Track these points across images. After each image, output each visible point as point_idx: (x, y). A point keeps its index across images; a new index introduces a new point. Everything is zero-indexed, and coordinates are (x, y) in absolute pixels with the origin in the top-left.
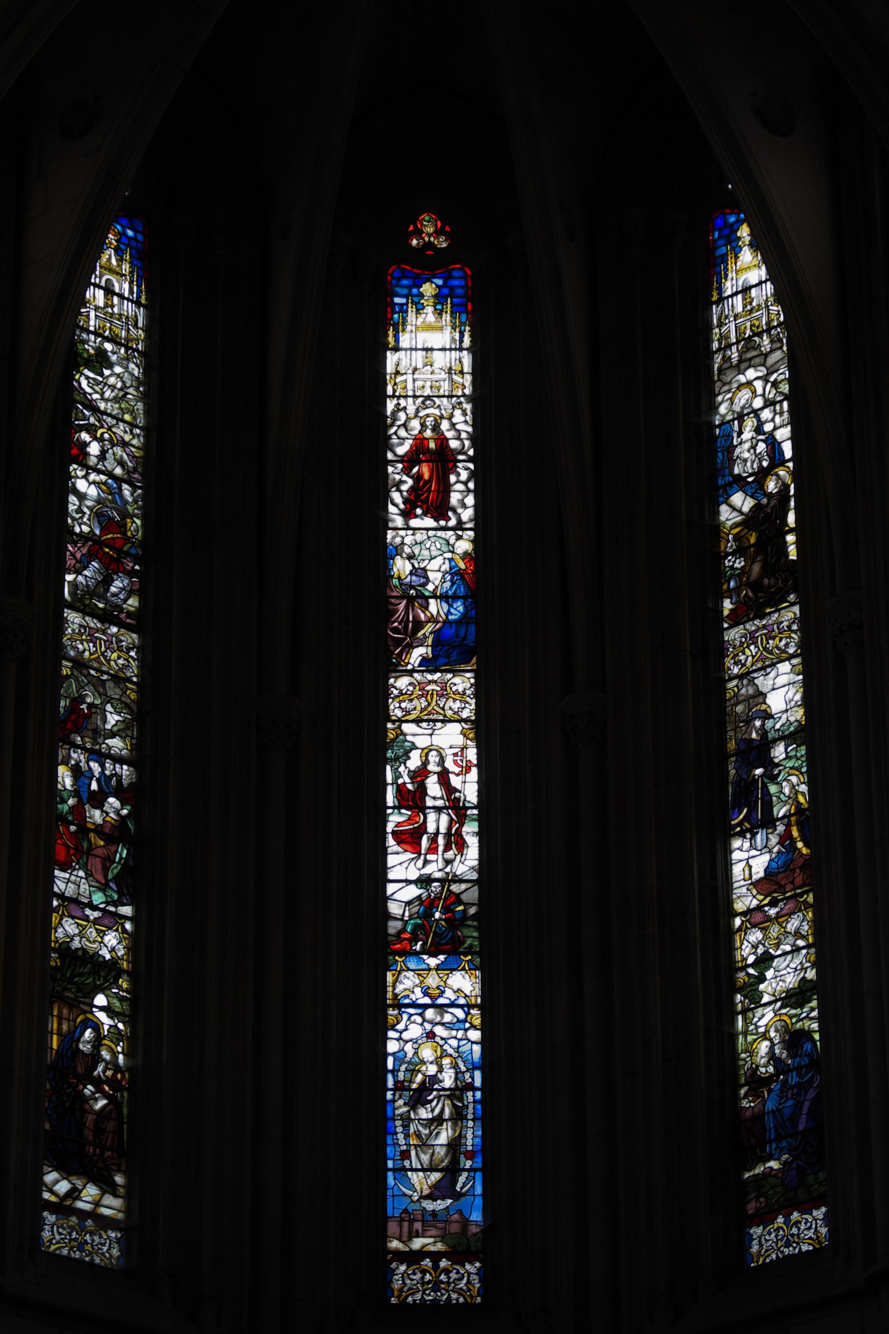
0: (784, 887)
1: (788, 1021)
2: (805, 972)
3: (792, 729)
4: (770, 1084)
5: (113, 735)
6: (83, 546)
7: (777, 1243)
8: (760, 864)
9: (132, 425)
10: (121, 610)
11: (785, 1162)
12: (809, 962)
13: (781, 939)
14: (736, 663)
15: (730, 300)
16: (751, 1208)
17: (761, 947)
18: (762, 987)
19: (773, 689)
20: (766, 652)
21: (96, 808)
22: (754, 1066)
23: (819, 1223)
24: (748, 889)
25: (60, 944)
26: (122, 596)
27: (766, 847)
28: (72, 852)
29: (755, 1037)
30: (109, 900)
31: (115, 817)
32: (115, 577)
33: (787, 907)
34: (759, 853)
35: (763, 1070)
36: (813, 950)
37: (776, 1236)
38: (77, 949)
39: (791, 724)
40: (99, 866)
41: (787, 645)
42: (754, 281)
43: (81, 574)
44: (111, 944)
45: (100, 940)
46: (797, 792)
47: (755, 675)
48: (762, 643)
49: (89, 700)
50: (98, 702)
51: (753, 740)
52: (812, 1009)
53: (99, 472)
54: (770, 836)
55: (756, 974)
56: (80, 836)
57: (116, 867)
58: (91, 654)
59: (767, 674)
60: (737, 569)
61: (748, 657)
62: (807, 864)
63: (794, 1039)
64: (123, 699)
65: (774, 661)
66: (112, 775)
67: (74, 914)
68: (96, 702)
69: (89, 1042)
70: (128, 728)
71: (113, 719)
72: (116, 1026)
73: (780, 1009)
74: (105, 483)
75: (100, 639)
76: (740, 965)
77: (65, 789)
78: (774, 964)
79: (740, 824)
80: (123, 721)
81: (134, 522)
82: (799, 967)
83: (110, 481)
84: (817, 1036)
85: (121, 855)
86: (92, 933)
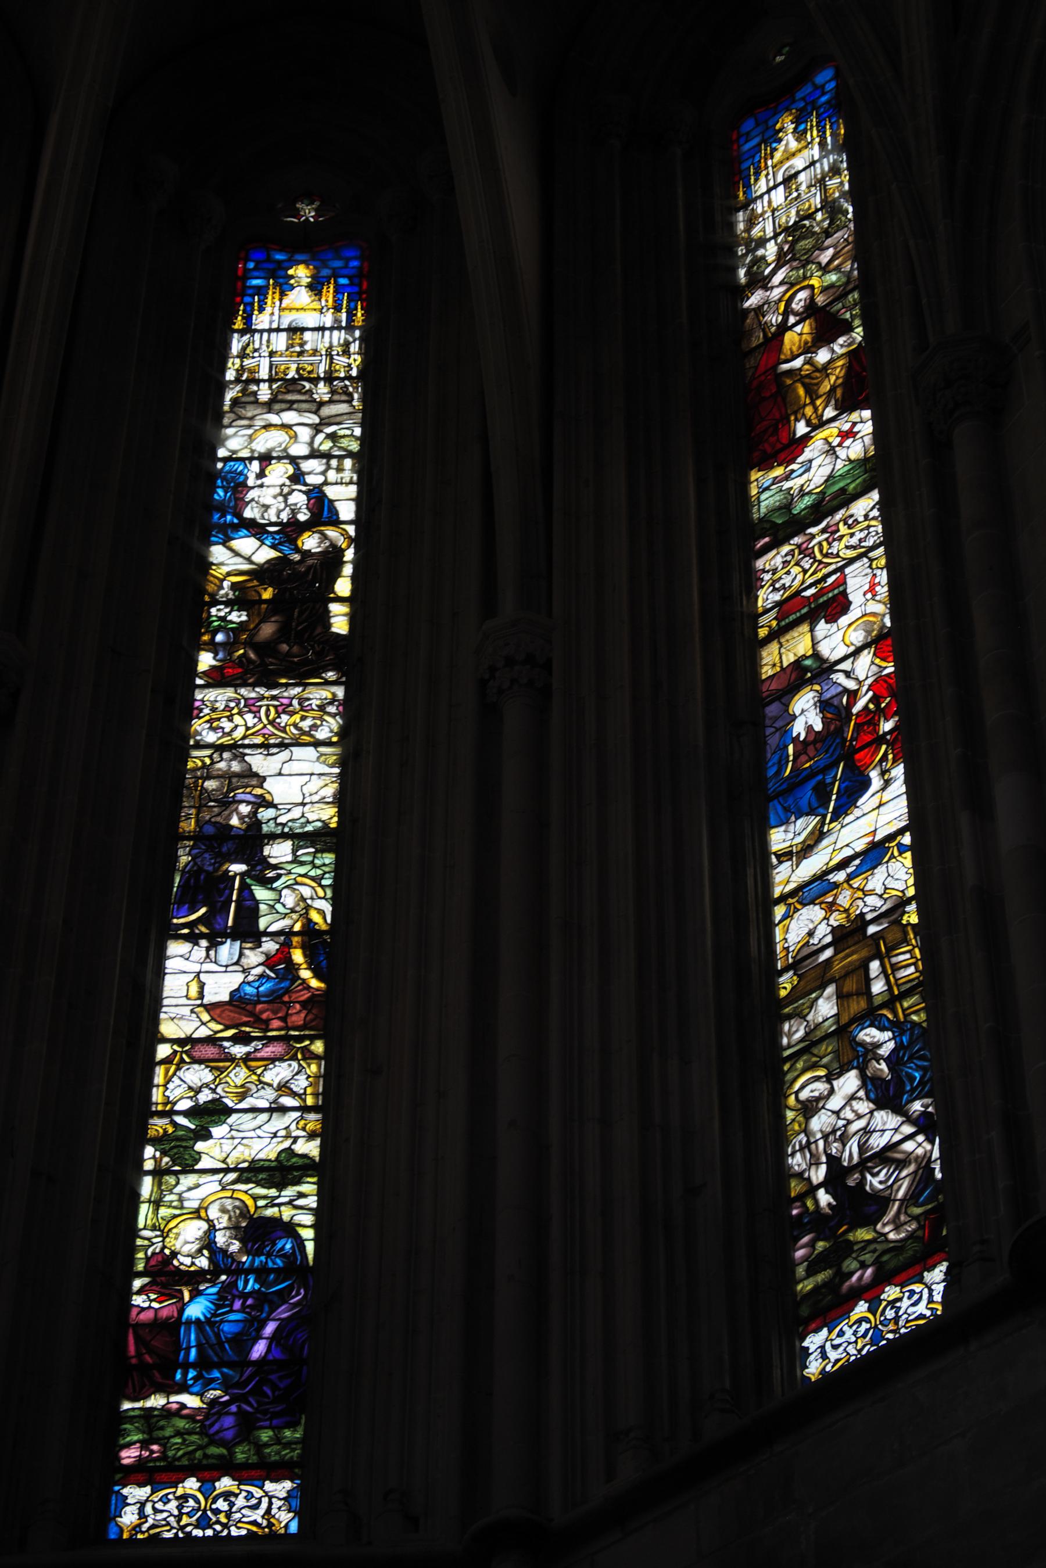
0: (267, 1022)
1: (250, 1202)
2: (294, 1142)
3: (309, 828)
4: (199, 1283)
7: (179, 1519)
8: (221, 987)
11: (214, 1402)
12: (304, 1129)
13: (249, 1089)
14: (212, 729)
15: (265, 335)
16: (129, 1456)
17: (206, 1091)
18: (200, 1146)
19: (280, 774)
20: (274, 726)
22: (167, 1252)
23: (277, 1503)
24: (192, 1011)
27: (237, 963)
29: (177, 1212)
33: (268, 1049)
34: (224, 969)
35: (188, 1261)
36: (312, 1116)
37: (180, 1507)
39: (308, 822)
41: (314, 727)
42: (311, 324)
46: (308, 908)
47: (247, 751)
48: (267, 716)
51: (233, 827)
52: (301, 1195)
54: (247, 952)
55: (193, 1127)
59: (268, 755)
60: (232, 622)
61: (236, 726)
62: (313, 1001)
63: (258, 1231)
65: (286, 741)
73: (234, 1182)
76: (160, 1108)
78: (230, 1120)
79: (190, 925)
82: (283, 1133)
84: (307, 1234)
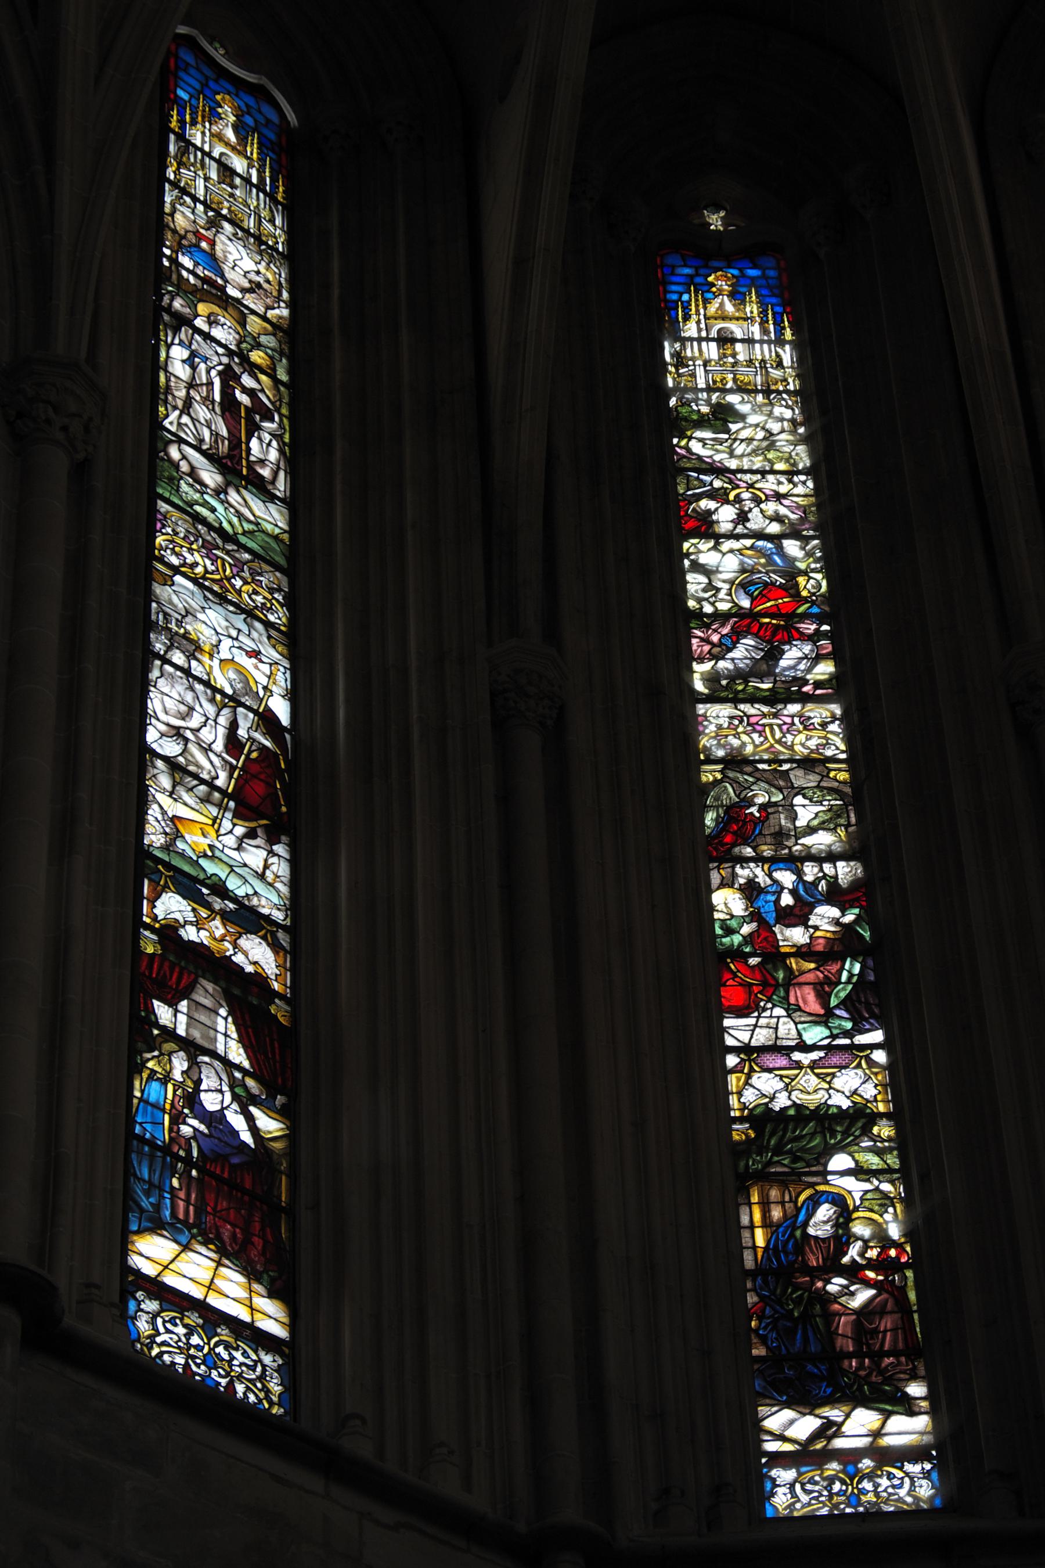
5: (810, 830)
6: (723, 625)
9: (790, 474)
10: (806, 682)
21: (794, 926)
25: (751, 1110)
26: (802, 667)
28: (755, 989)
30: (835, 1032)
31: (833, 929)
32: (786, 647)
38: (784, 1110)
40: (811, 997)
43: (723, 658)
44: (851, 1086)
45: (826, 1086)
49: (760, 800)
50: (778, 797)
53: (738, 537)
56: (769, 966)
57: (844, 989)
58: (756, 746)
64: (823, 784)
66: (818, 880)
67: (771, 1066)
68: (773, 799)
69: (825, 1222)
70: (839, 816)
71: (806, 813)
72: (877, 1189)
74: (752, 547)
75: (771, 726)
77: (732, 916)
80: (829, 810)
81: (810, 578)
83: (760, 543)
85: (849, 972)
86: (810, 1081)
